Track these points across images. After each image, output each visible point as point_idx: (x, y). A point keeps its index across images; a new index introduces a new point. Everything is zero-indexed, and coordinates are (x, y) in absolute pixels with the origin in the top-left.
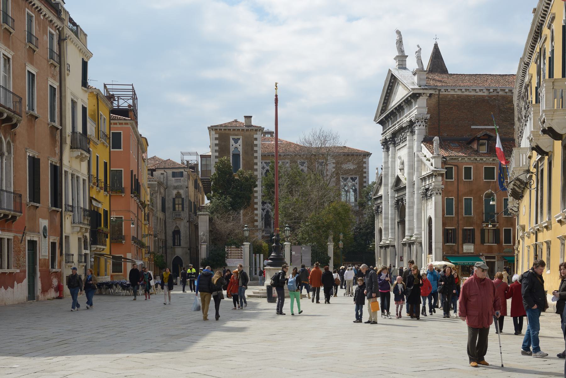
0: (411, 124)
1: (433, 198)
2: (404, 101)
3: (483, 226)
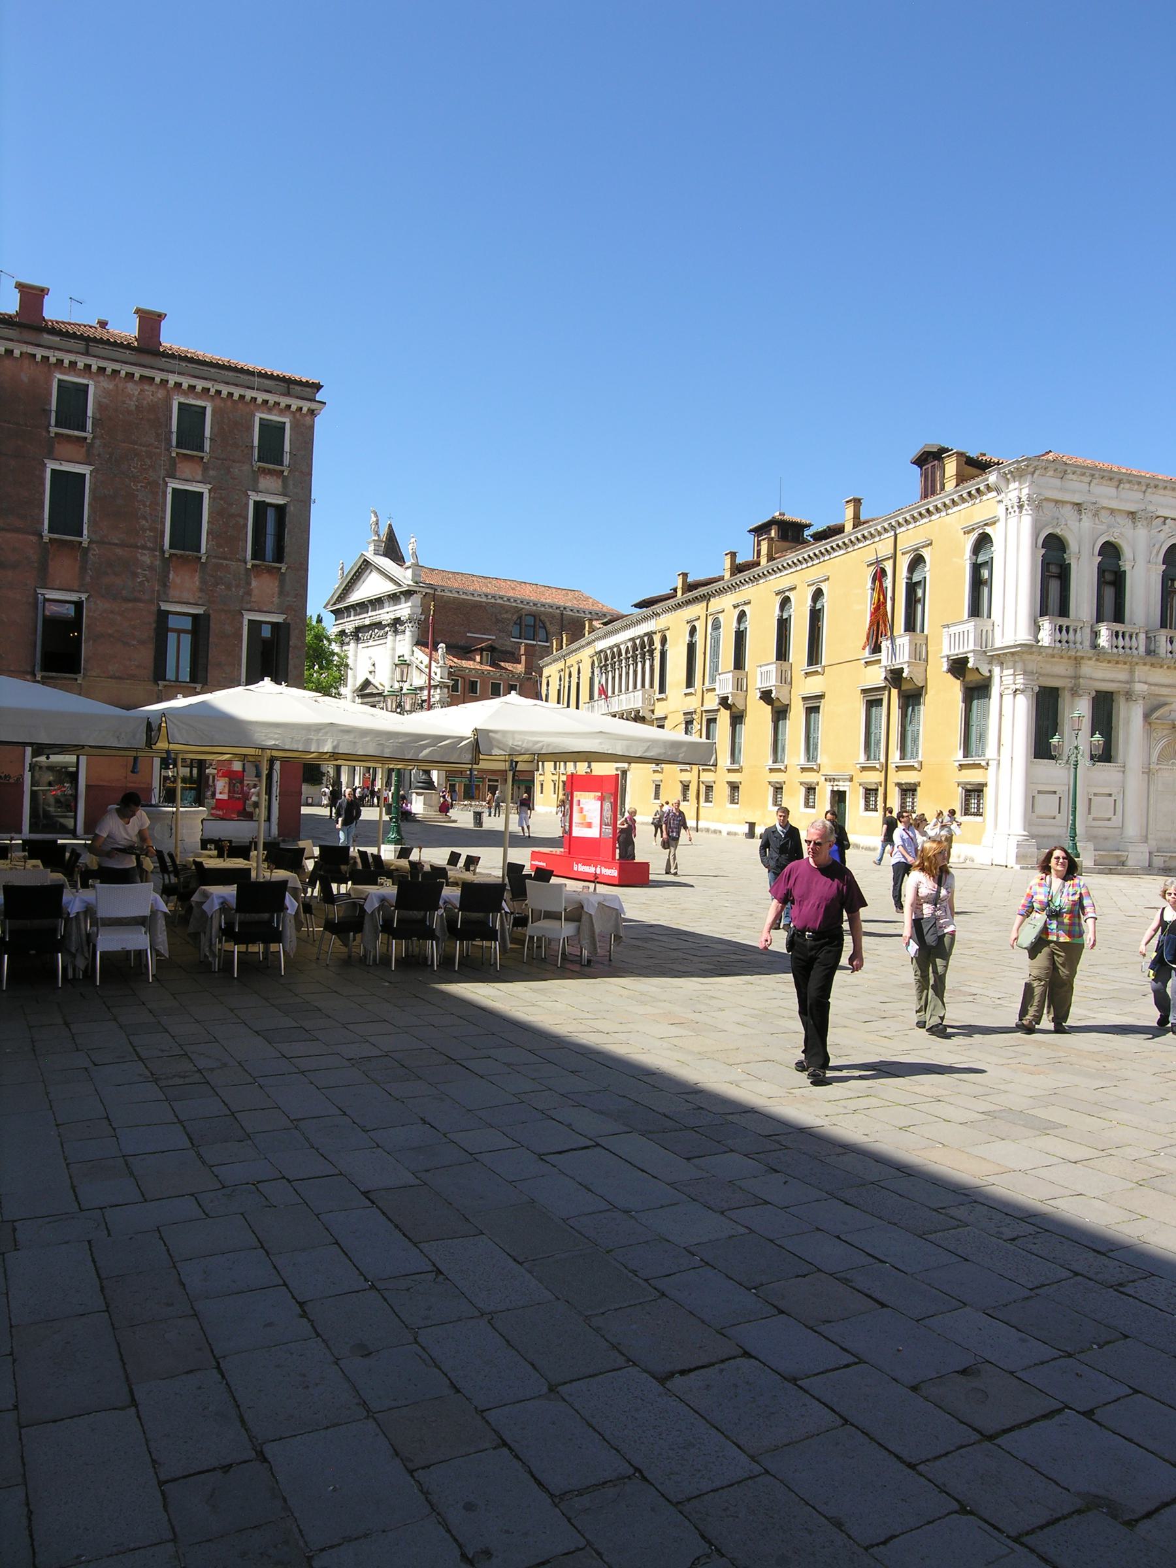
0: (397, 621)
2: (389, 595)
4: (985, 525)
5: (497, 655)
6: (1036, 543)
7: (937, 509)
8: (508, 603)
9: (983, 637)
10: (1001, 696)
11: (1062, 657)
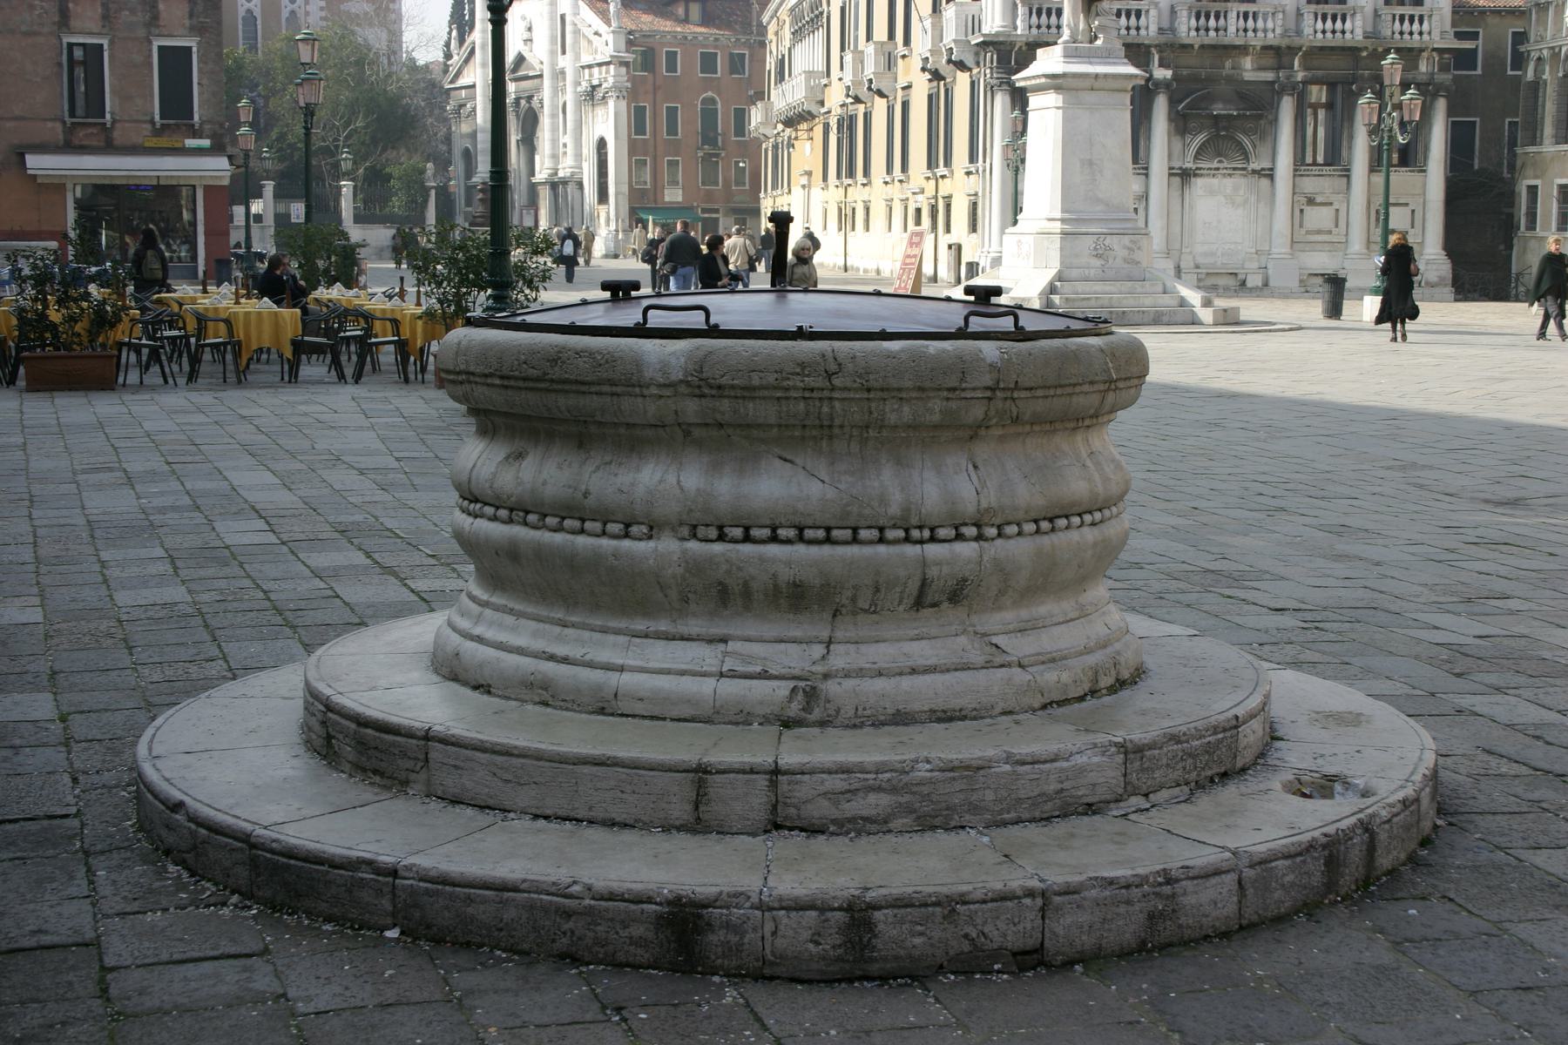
1: (611, 103)
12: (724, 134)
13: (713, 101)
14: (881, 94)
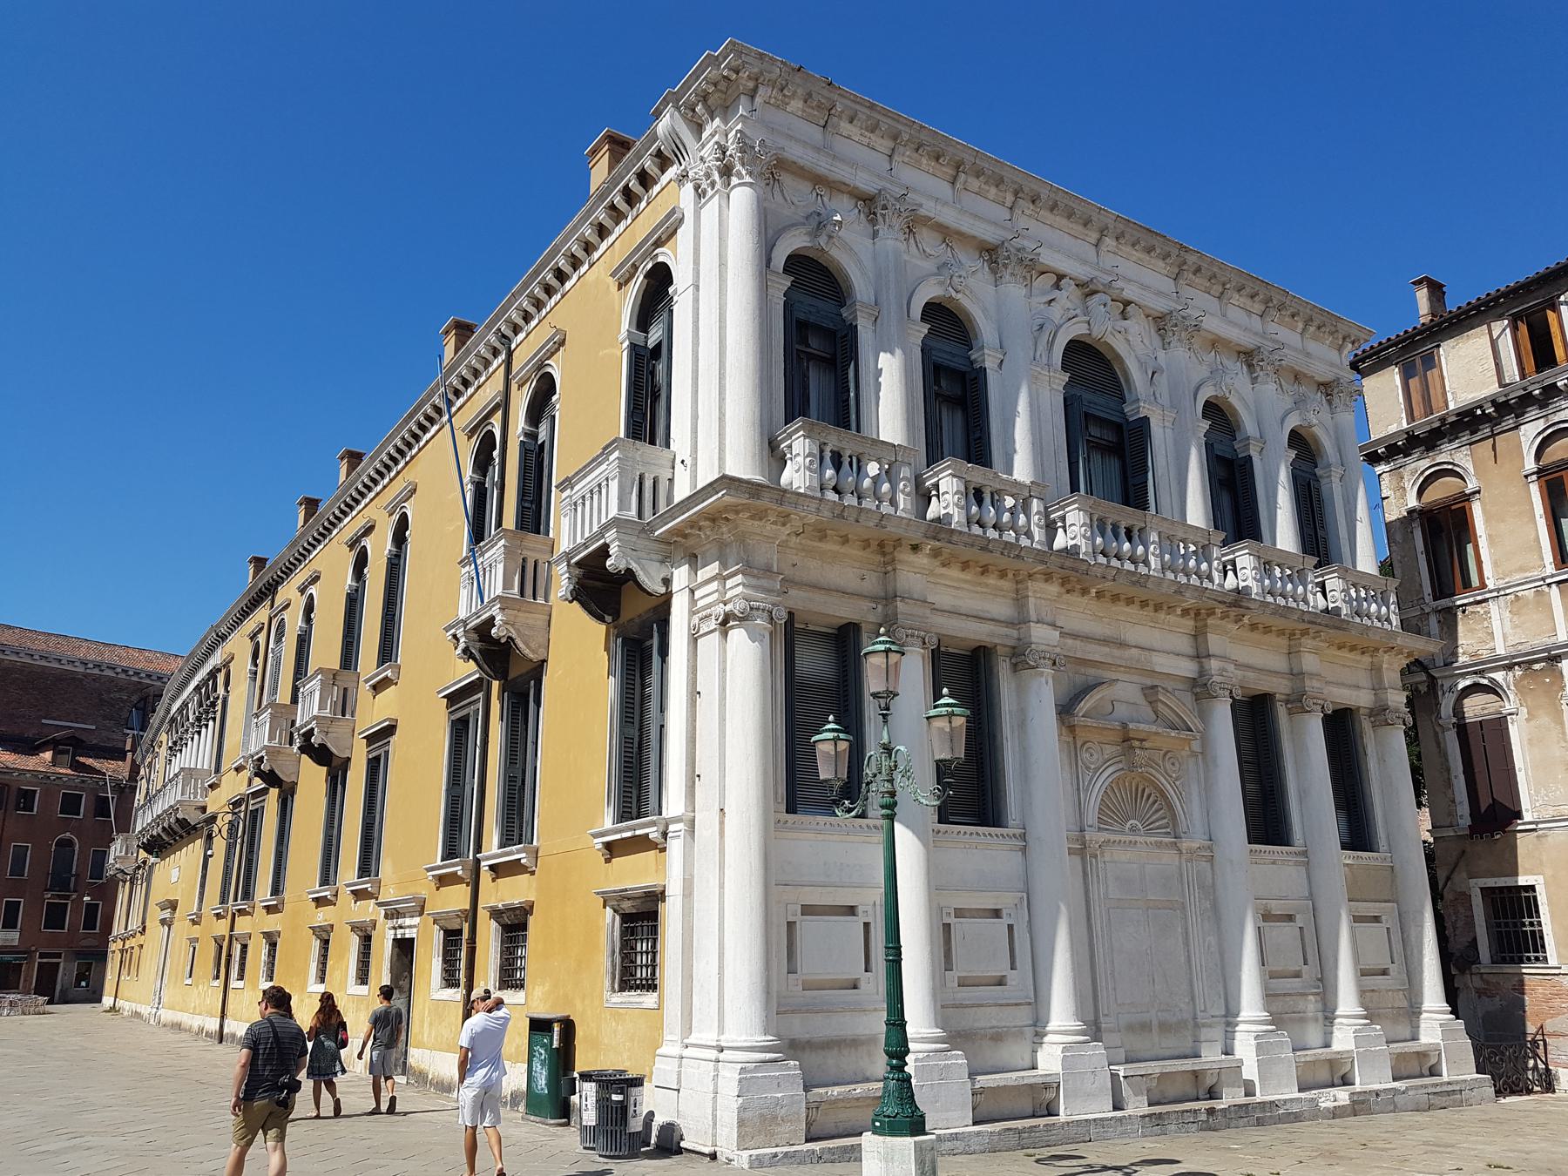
3: (46, 896)
4: (659, 243)
5: (71, 747)
6: (769, 261)
7: (576, 263)
8: (124, 676)
9: (646, 490)
10: (694, 639)
11: (845, 540)
12: (77, 875)
13: (70, 843)
14: (321, 755)
